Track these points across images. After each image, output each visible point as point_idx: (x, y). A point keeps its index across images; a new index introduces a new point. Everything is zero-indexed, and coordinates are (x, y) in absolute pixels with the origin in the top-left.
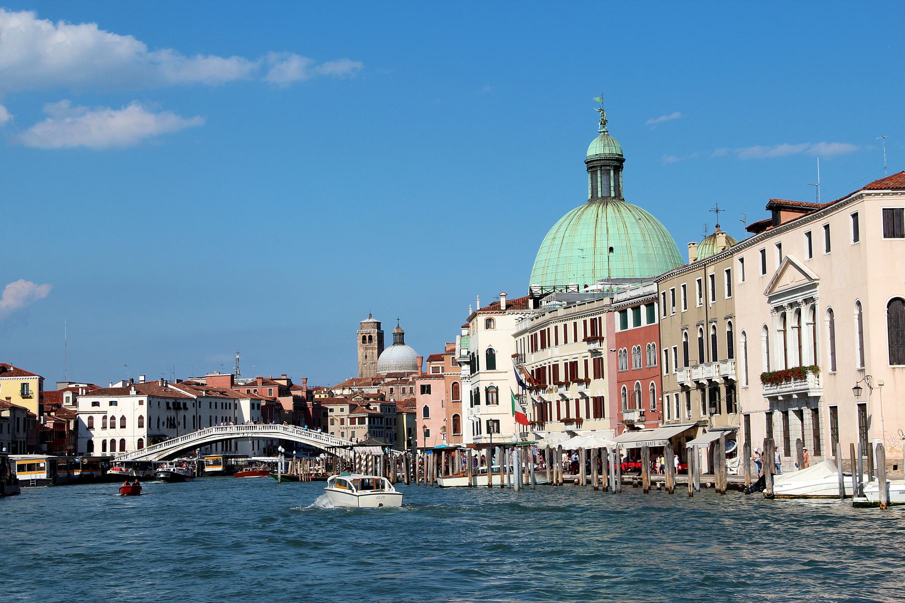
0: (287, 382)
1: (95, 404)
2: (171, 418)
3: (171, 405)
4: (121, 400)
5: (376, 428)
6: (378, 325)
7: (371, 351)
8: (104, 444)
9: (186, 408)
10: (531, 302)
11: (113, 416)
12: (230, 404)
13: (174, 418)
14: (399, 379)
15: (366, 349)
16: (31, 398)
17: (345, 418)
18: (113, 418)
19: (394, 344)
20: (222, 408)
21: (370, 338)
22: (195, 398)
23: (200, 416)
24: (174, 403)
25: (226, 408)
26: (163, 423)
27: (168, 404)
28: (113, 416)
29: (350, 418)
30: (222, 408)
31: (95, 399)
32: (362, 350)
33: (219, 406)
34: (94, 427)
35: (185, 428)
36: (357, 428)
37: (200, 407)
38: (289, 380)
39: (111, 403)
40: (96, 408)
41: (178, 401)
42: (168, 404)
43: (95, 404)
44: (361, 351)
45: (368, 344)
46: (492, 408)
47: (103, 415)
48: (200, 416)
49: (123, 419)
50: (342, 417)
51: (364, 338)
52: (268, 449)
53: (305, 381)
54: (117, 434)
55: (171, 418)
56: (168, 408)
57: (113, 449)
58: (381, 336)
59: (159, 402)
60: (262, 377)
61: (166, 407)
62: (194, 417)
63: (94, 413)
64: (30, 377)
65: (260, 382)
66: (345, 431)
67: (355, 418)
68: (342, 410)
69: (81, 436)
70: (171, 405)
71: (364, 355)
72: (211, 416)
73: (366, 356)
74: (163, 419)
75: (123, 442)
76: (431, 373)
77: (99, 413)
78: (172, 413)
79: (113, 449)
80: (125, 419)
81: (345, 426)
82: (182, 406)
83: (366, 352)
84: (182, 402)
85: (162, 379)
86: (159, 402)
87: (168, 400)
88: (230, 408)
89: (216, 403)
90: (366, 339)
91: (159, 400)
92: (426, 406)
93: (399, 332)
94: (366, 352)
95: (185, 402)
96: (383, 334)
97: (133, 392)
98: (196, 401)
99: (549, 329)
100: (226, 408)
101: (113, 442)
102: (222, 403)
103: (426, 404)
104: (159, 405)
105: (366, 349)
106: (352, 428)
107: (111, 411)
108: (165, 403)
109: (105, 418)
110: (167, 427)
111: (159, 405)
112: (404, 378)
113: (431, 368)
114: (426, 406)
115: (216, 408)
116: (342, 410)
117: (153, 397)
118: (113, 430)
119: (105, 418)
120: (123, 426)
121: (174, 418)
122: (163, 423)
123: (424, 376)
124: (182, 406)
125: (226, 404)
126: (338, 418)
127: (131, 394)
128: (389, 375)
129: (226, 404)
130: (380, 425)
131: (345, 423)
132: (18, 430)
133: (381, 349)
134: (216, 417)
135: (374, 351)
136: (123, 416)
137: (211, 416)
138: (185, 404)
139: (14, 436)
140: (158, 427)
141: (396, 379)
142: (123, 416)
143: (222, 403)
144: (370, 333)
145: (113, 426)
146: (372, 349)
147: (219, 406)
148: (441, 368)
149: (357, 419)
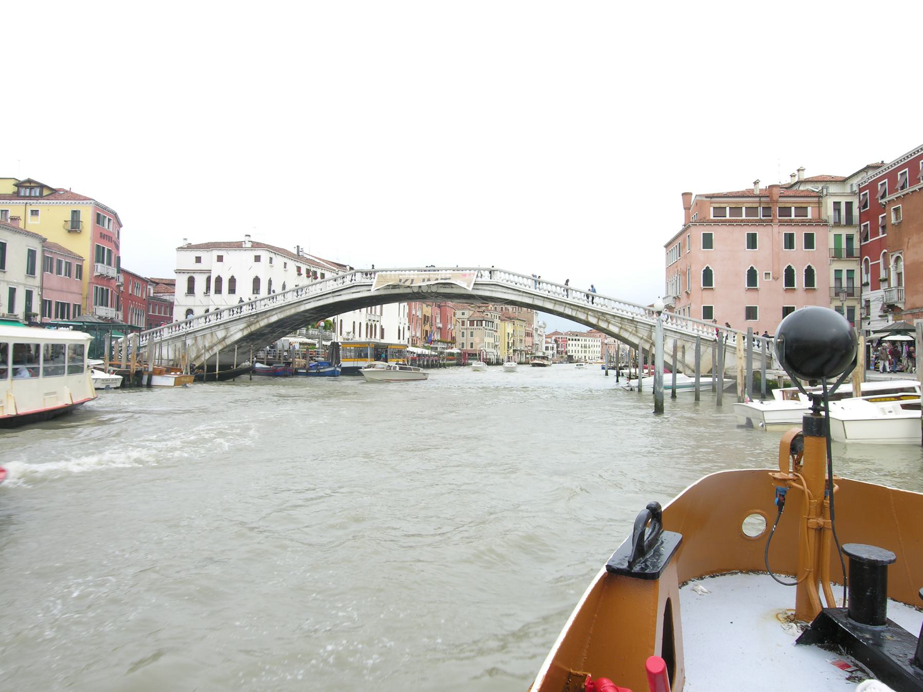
3: (303, 271)
4: (228, 255)
5: (490, 330)
11: (219, 276)
17: (466, 320)
18: (219, 280)
22: (337, 270)
24: (308, 271)
27: (299, 269)
28: (219, 276)
29: (470, 321)
31: (198, 254)
34: (195, 292)
41: (313, 269)
42: (299, 269)
49: (232, 281)
50: (463, 320)
59: (285, 264)
61: (297, 273)
63: (195, 271)
64: (81, 202)
66: (465, 331)
67: (474, 321)
68: (463, 314)
70: (303, 271)
76: (712, 217)
77: (201, 272)
80: (235, 282)
81: (465, 327)
85: (298, 246)
86: (285, 264)
91: (286, 260)
92: (707, 268)
95: (323, 272)
103: (708, 265)
104: (285, 267)
106: (471, 329)
108: (296, 268)
109: (209, 279)
111: (285, 267)
113: (712, 209)
114: (707, 268)
116: (463, 314)
118: (218, 296)
119: (209, 279)
120: (232, 290)
123: (703, 222)
126: (460, 321)
127: (243, 246)
130: (491, 328)
136: (233, 277)
142: (233, 277)
145: (218, 291)
148: (728, 209)
149: (475, 322)
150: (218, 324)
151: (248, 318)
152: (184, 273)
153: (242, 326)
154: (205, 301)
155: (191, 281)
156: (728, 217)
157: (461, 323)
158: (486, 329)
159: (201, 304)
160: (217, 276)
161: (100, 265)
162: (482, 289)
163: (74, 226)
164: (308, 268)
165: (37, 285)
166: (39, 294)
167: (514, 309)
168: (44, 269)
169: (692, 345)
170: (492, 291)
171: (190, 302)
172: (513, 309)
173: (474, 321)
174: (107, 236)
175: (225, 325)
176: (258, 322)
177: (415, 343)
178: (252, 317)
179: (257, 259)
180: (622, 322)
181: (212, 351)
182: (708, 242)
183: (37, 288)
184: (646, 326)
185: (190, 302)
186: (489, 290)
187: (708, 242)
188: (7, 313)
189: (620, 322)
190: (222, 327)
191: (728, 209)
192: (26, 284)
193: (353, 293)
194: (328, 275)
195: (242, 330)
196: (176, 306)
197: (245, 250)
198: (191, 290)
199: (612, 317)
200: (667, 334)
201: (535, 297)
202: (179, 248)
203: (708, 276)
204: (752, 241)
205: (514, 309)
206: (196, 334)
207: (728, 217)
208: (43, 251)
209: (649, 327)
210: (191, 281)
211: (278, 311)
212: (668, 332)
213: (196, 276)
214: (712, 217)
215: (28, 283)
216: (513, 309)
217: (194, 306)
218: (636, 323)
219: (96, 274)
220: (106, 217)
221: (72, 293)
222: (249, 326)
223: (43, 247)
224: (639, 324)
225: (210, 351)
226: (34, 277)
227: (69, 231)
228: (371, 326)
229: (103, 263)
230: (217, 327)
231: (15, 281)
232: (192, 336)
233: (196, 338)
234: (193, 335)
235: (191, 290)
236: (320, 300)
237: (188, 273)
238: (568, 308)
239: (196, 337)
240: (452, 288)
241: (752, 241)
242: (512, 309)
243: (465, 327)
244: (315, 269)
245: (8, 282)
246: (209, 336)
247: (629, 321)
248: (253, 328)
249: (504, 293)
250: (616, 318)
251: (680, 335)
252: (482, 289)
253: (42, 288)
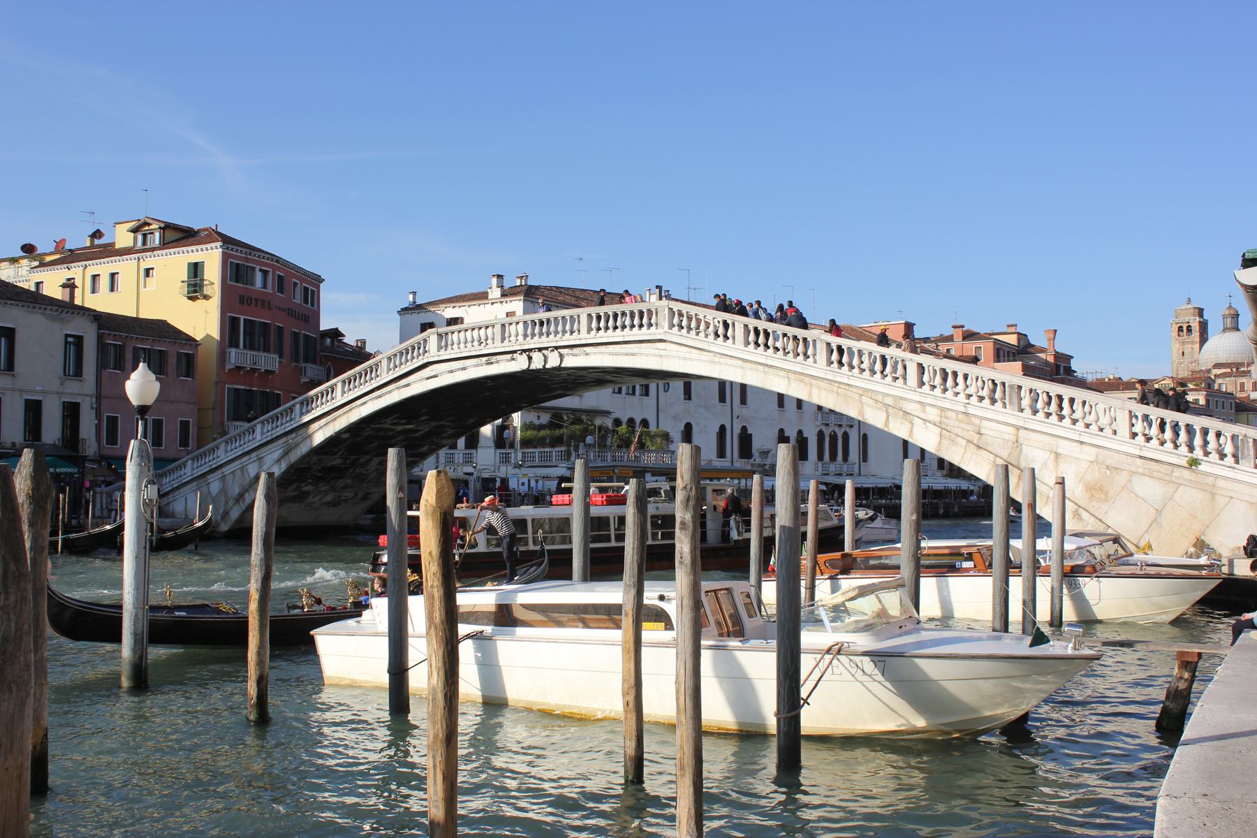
0: (1019, 339)
6: (1200, 312)
7: (1190, 346)
14: (1234, 370)
15: (1183, 343)
16: (206, 297)
19: (1225, 330)
21: (1189, 329)
38: (1022, 336)
44: (1176, 347)
45: (1185, 337)
51: (1180, 329)
53: (1052, 336)
58: (1204, 326)
60: (959, 324)
65: (958, 334)
71: (1181, 352)
90: (1182, 331)
93: (1232, 312)
96: (1207, 324)
97: (495, 293)
105: (1183, 343)
112: (1242, 369)
128: (1217, 366)
133: (1204, 339)
135: (1194, 346)
141: (1229, 370)
144: (1188, 322)
146: (1192, 343)
150: (246, 450)
151: (284, 439)
153: (276, 455)
161: (233, 351)
162: (642, 354)
163: (195, 288)
165: (90, 393)
166: (92, 408)
168: (101, 365)
169: (1130, 480)
170: (661, 356)
174: (256, 300)
175: (258, 452)
178: (290, 437)
180: (944, 420)
181: (244, 502)
183: (89, 398)
184: (1003, 428)
186: (655, 355)
188: (22, 441)
189: (937, 419)
190: (254, 455)
192: (63, 393)
193: (428, 378)
195: (279, 460)
197: (492, 304)
199: (918, 407)
200: (1059, 451)
201: (745, 365)
202: (403, 309)
206: (224, 469)
208: (100, 337)
209: (1012, 430)
212: (1062, 442)
215: (66, 391)
218: (977, 421)
219: (228, 367)
220: (255, 268)
221: (172, 402)
222: (286, 453)
223: (99, 329)
224: (985, 423)
225: (241, 502)
226: (81, 381)
227: (190, 298)
228: (834, 438)
229: (237, 346)
230: (247, 458)
231: (38, 388)
232: (218, 474)
233: (223, 478)
234: (220, 472)
236: (380, 397)
238: (819, 387)
239: (224, 476)
240: (587, 354)
245: (21, 391)
246: (238, 473)
247: (960, 416)
248: (295, 456)
249: (685, 359)
250: (929, 409)
251: (1094, 450)
252: (642, 354)
253: (99, 397)
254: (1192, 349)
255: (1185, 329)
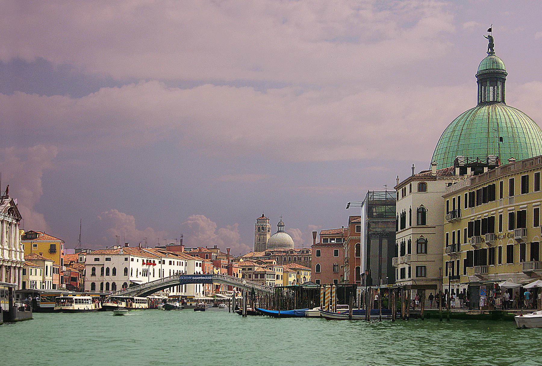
1: (97, 260)
2: (145, 270)
3: (145, 262)
4: (113, 258)
8: (102, 284)
9: (154, 264)
10: (458, 170)
12: (182, 262)
13: (147, 270)
17: (252, 274)
18: (108, 269)
20: (178, 265)
21: (263, 228)
23: (163, 270)
25: (180, 265)
26: (140, 273)
30: (178, 265)
32: (257, 236)
33: (176, 263)
35: (154, 277)
36: (259, 280)
37: (164, 263)
39: (107, 259)
40: (97, 262)
41: (149, 259)
43: (97, 260)
46: (423, 258)
47: (101, 267)
48: (163, 270)
49: (114, 270)
50: (249, 274)
52: (205, 292)
54: (109, 279)
55: (145, 270)
56: (143, 264)
57: (108, 289)
59: (138, 260)
61: (142, 263)
62: (160, 269)
69: (86, 280)
70: (145, 262)
71: (259, 238)
72: (170, 270)
73: (260, 239)
74: (140, 270)
75: (114, 285)
76: (322, 243)
78: (145, 267)
79: (108, 289)
82: (152, 262)
83: (260, 237)
84: (152, 260)
86: (138, 260)
87: (143, 259)
88: (182, 265)
89: (174, 262)
94: (260, 237)
95: (154, 260)
98: (161, 260)
99: (459, 197)
100: (180, 265)
101: (108, 284)
102: (178, 262)
105: (260, 235)
107: (107, 264)
110: (143, 276)
115: (174, 264)
117: (134, 256)
121: (147, 270)
122: (140, 273)
124: (152, 262)
125: (180, 262)
129: (180, 262)
131: (252, 277)
132: (47, 274)
134: (174, 270)
136: (114, 268)
137: (170, 270)
138: (154, 261)
139: (44, 278)
140: (137, 276)
142: (114, 268)
143: (178, 262)
145: (108, 274)
147: (176, 263)
148: (329, 239)
149: (259, 275)
152: (90, 266)
154: (101, 278)
155: (94, 269)
156: (329, 243)
157: (248, 276)
158: (268, 280)
159: (98, 280)
160: (107, 267)
164: (147, 259)
167: (306, 258)
171: (93, 279)
172: (305, 259)
173: (258, 274)
176: (141, 292)
177: (208, 293)
179: (126, 259)
182: (318, 254)
185: (93, 279)
187: (318, 254)
191: (329, 239)
194: (157, 261)
196: (86, 281)
198: (93, 274)
203: (318, 267)
204: (336, 253)
205: (306, 258)
207: (329, 243)
210: (94, 269)
211: (147, 289)
213: (95, 267)
214: (322, 243)
216: (305, 259)
217: (95, 281)
235: (93, 274)
237: (92, 266)
241: (336, 253)
242: (304, 259)
243: (251, 279)
244: (150, 259)
254: (263, 237)
255: (261, 228)
